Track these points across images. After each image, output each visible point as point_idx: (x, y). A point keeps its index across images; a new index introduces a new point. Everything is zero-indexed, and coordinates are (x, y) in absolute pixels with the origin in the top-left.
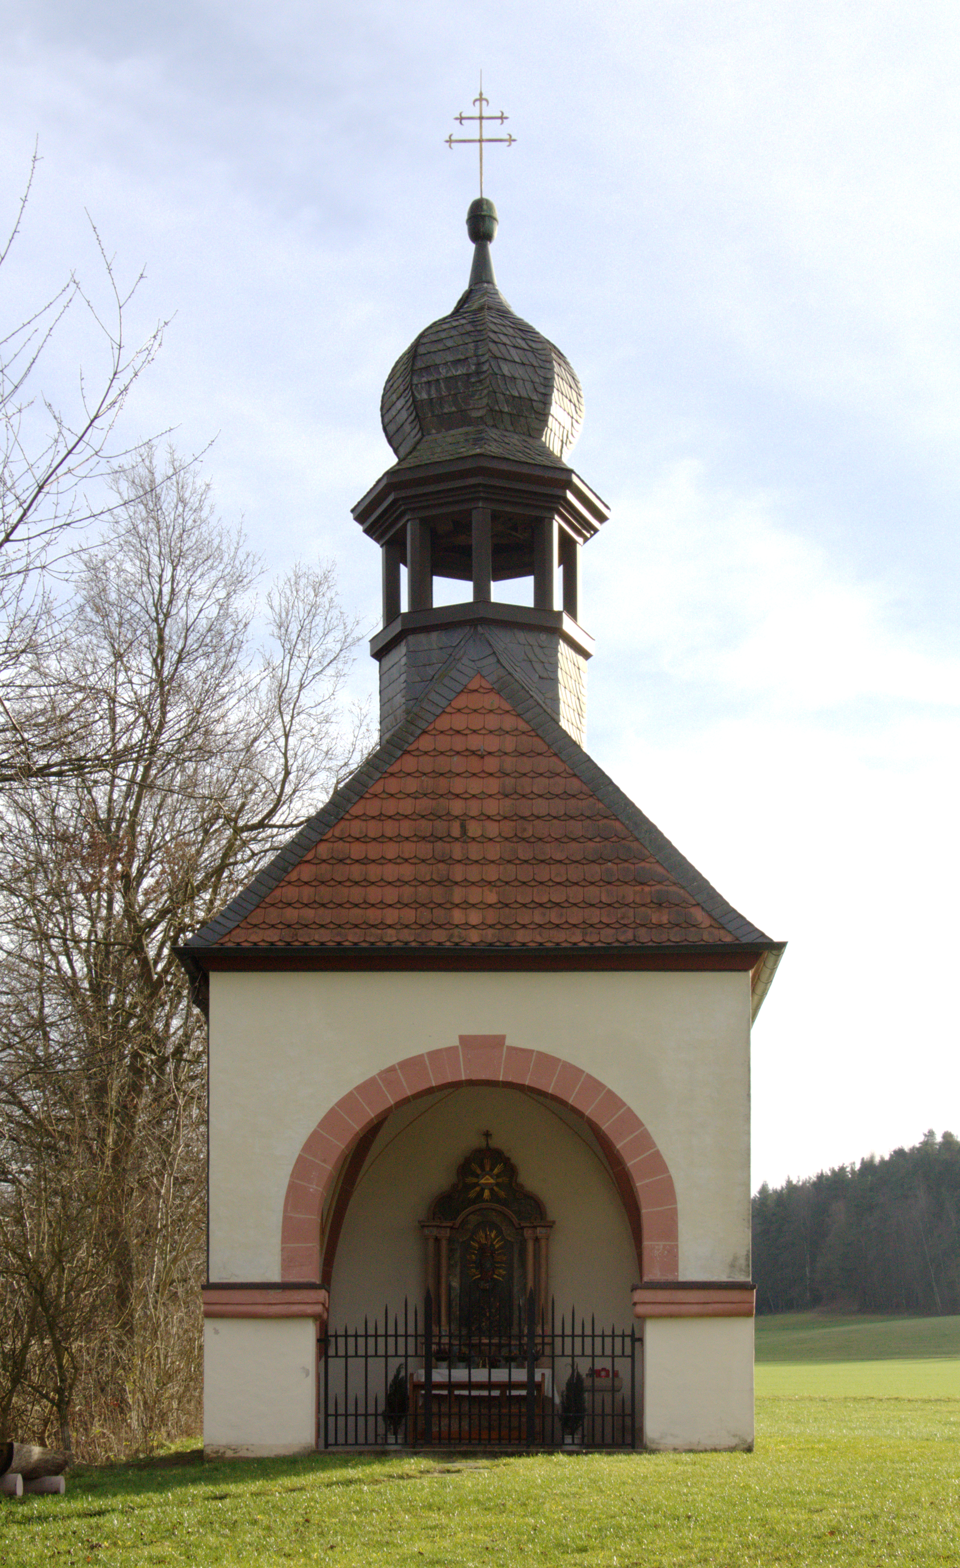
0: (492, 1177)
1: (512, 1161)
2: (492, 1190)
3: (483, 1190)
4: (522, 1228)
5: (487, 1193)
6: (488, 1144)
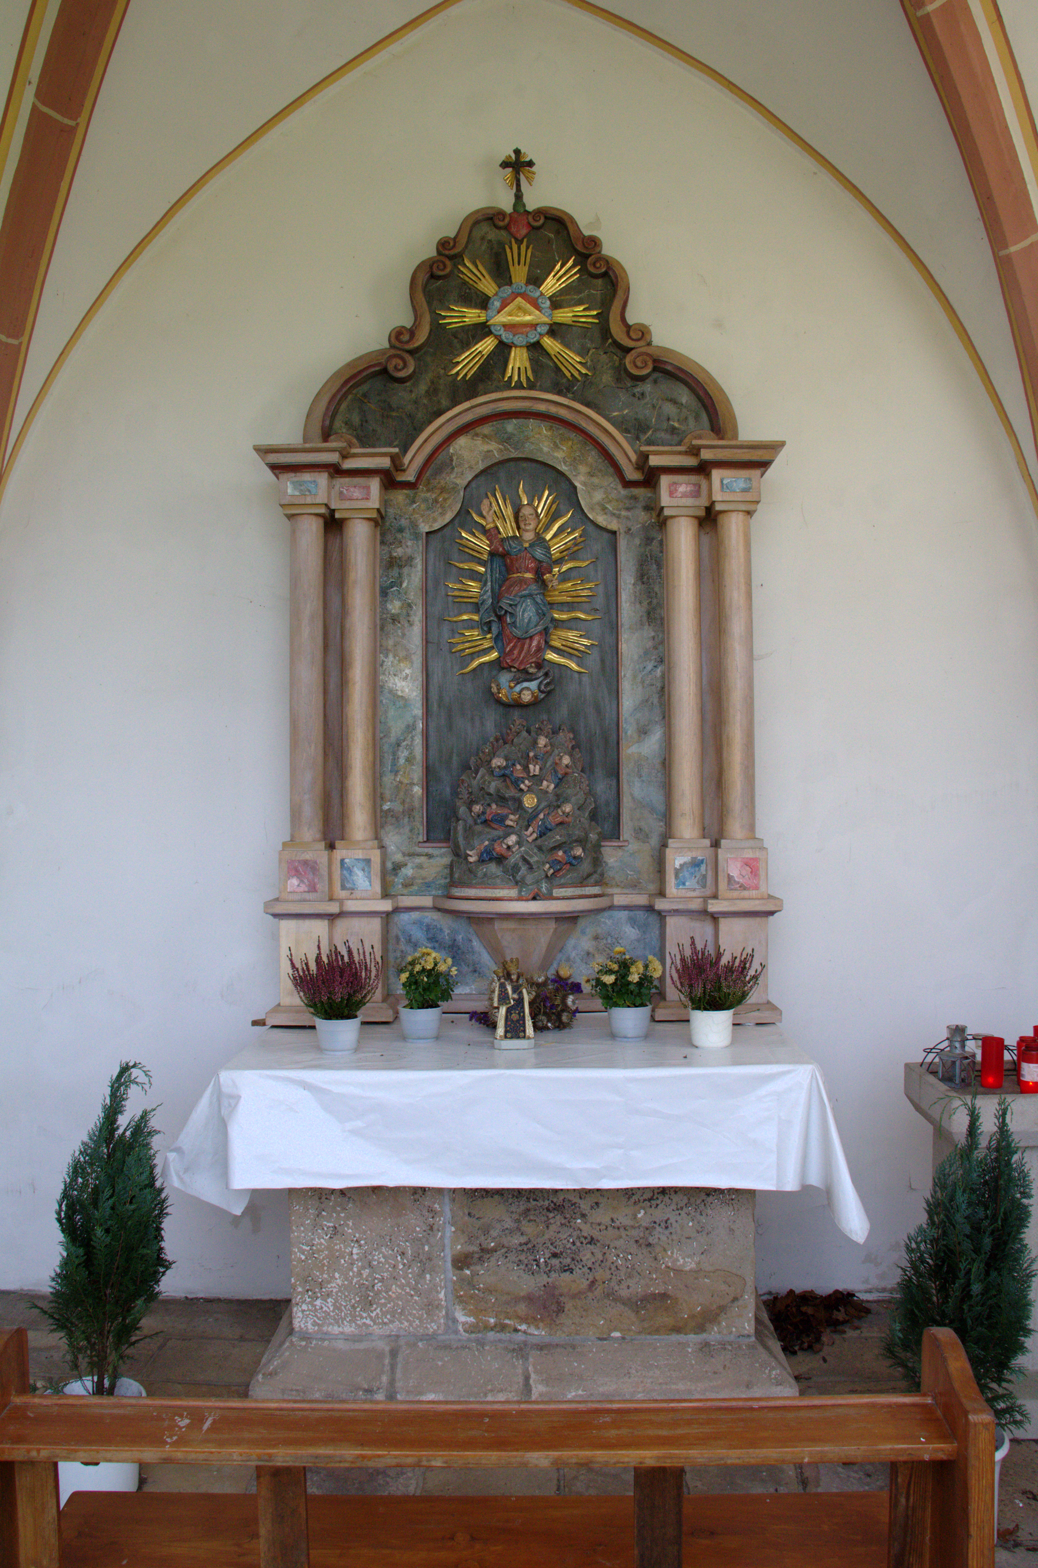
1: (608, 249)
2: (535, 347)
3: (503, 349)
4: (650, 478)
5: (518, 361)
6: (519, 196)
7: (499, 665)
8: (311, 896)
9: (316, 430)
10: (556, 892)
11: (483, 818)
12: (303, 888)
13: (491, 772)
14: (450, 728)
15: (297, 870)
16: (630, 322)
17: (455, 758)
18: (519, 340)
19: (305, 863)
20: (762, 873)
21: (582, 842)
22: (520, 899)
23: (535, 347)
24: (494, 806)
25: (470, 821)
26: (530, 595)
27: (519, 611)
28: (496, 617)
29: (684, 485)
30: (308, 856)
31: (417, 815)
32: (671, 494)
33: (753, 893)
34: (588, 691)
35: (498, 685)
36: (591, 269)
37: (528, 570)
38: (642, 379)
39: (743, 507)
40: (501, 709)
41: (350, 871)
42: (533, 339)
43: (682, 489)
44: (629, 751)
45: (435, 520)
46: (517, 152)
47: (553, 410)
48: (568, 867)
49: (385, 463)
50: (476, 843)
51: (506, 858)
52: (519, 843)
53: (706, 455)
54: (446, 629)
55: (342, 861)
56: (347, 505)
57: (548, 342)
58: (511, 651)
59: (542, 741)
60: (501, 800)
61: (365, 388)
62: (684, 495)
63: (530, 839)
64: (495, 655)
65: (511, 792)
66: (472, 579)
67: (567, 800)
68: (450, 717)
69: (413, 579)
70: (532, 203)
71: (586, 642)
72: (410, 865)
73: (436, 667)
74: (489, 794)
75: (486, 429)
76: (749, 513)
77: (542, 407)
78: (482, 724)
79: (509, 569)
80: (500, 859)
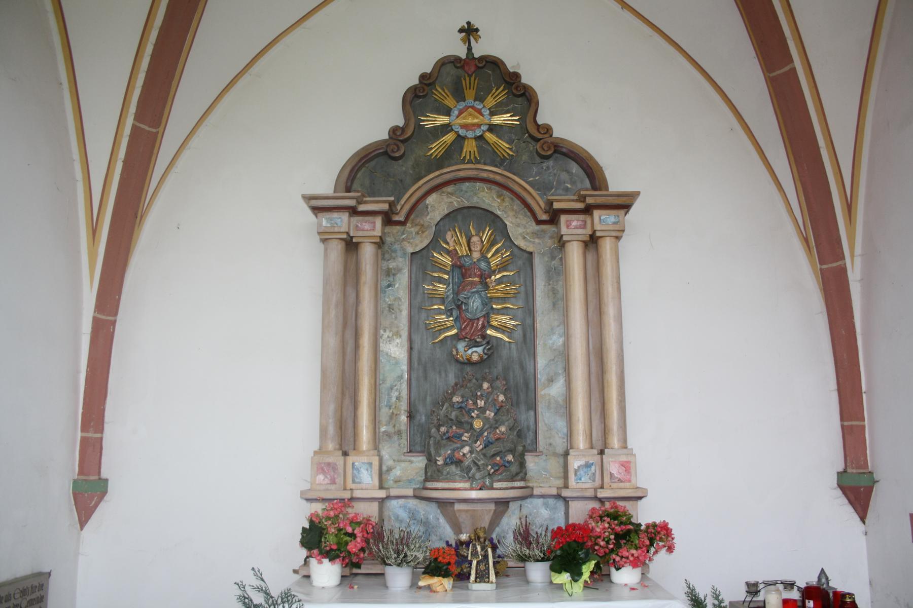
0: (479, 112)
1: (524, 80)
4: (554, 217)
5: (470, 147)
6: (470, 49)
7: (457, 338)
8: (332, 487)
9: (342, 186)
10: (496, 485)
11: (447, 435)
12: (327, 481)
13: (452, 405)
14: (426, 378)
15: (322, 469)
16: (540, 122)
17: (429, 399)
18: (470, 134)
19: (329, 464)
20: (633, 471)
21: (512, 451)
22: (472, 489)
23: (481, 138)
24: (454, 428)
25: (438, 438)
26: (477, 292)
27: (471, 301)
28: (457, 306)
29: (576, 220)
30: (331, 460)
31: (404, 435)
32: (568, 227)
33: (628, 485)
34: (515, 353)
35: (457, 350)
36: (514, 91)
37: (476, 276)
38: (547, 158)
39: (614, 234)
40: (458, 366)
41: (358, 470)
42: (478, 133)
43: (574, 223)
44: (543, 393)
45: (416, 245)
46: (469, 23)
47: (491, 176)
48: (502, 469)
49: (385, 207)
50: (442, 452)
51: (462, 462)
52: (471, 452)
53: (590, 201)
54: (423, 315)
55: (353, 464)
56: (360, 233)
57: (489, 136)
58: (465, 327)
59: (486, 385)
60: (460, 424)
61: (373, 163)
62: (576, 228)
63: (478, 449)
64: (454, 331)
65: (466, 418)
66: (440, 283)
67: (502, 423)
68: (425, 371)
69: (402, 281)
70: (478, 53)
71: (514, 323)
72: (398, 468)
73: (417, 338)
74: (452, 420)
75: (450, 189)
76: (618, 238)
77: (485, 175)
78: (446, 376)
79: (464, 276)
80: (458, 463)
